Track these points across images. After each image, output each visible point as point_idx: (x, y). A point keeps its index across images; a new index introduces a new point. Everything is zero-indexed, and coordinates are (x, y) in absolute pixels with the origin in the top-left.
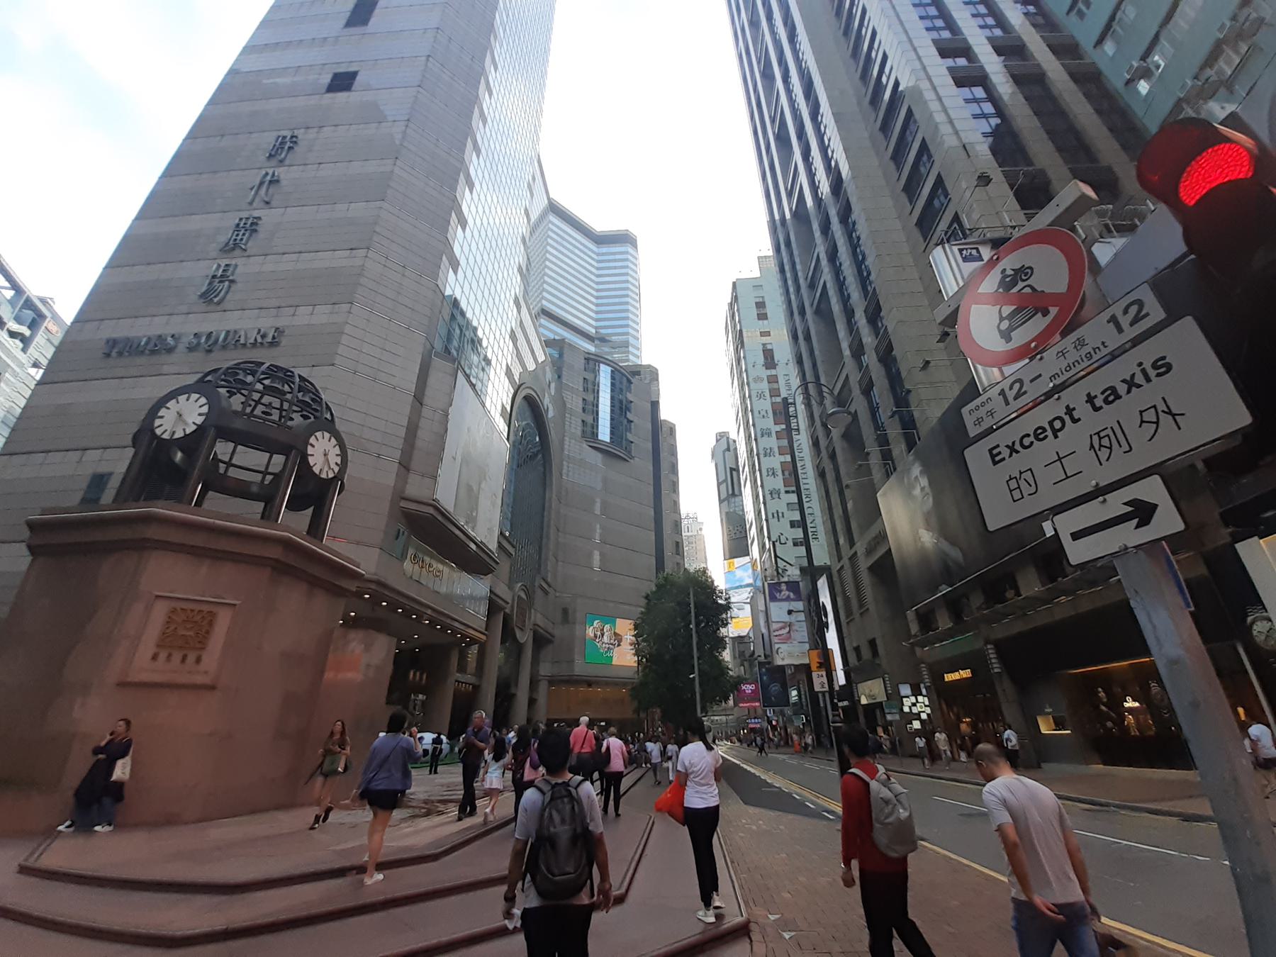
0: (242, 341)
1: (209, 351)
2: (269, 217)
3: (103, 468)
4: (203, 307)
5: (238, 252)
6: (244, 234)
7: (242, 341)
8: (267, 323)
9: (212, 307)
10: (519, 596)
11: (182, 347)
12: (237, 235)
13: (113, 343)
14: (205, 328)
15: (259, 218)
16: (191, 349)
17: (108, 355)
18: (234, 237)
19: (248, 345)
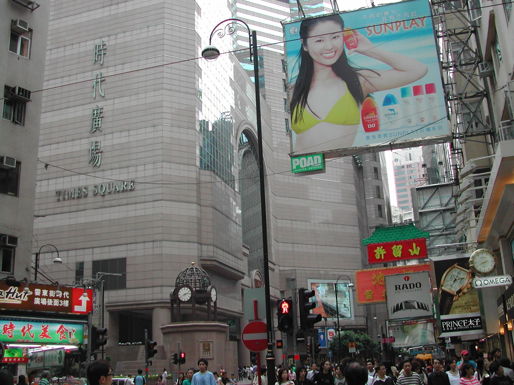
0: (118, 190)
1: (104, 196)
2: (107, 106)
3: (80, 259)
4: (90, 169)
5: (98, 132)
6: (99, 121)
7: (118, 190)
8: (124, 177)
9: (96, 169)
10: (255, 279)
11: (91, 194)
12: (96, 121)
13: (58, 193)
14: (98, 181)
15: (103, 108)
16: (95, 195)
17: (59, 200)
18: (94, 123)
19: (121, 191)
